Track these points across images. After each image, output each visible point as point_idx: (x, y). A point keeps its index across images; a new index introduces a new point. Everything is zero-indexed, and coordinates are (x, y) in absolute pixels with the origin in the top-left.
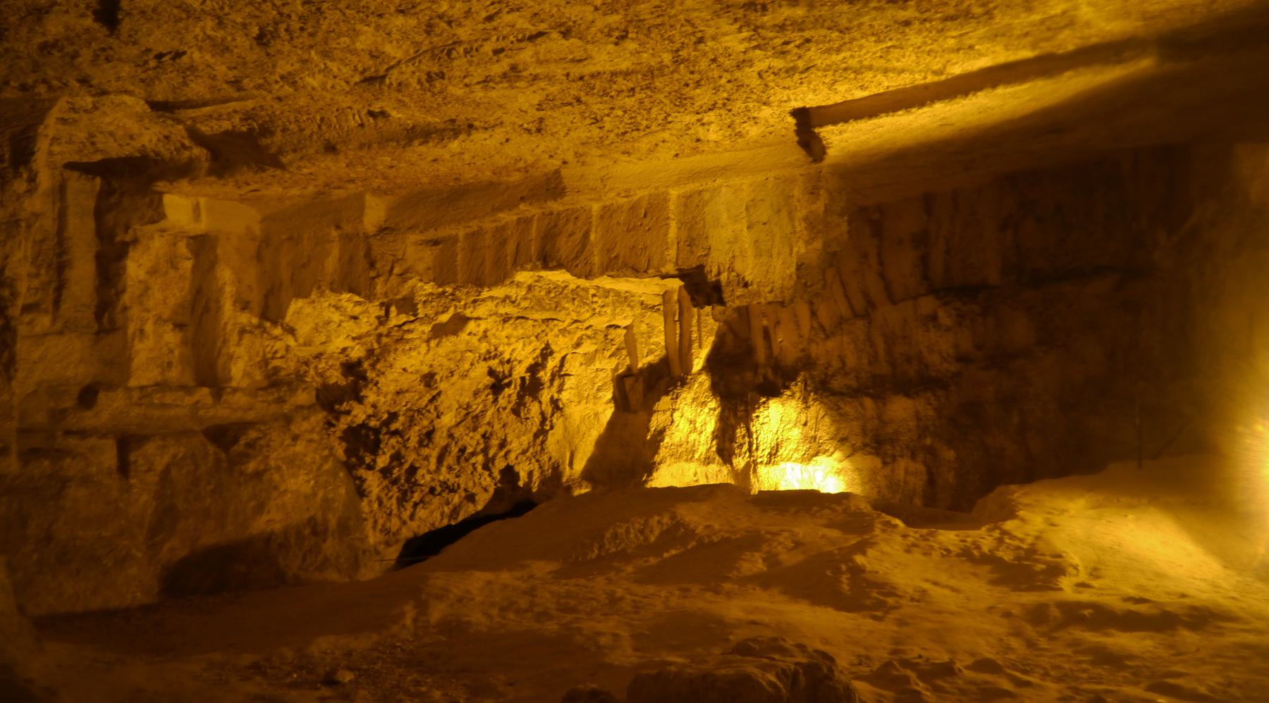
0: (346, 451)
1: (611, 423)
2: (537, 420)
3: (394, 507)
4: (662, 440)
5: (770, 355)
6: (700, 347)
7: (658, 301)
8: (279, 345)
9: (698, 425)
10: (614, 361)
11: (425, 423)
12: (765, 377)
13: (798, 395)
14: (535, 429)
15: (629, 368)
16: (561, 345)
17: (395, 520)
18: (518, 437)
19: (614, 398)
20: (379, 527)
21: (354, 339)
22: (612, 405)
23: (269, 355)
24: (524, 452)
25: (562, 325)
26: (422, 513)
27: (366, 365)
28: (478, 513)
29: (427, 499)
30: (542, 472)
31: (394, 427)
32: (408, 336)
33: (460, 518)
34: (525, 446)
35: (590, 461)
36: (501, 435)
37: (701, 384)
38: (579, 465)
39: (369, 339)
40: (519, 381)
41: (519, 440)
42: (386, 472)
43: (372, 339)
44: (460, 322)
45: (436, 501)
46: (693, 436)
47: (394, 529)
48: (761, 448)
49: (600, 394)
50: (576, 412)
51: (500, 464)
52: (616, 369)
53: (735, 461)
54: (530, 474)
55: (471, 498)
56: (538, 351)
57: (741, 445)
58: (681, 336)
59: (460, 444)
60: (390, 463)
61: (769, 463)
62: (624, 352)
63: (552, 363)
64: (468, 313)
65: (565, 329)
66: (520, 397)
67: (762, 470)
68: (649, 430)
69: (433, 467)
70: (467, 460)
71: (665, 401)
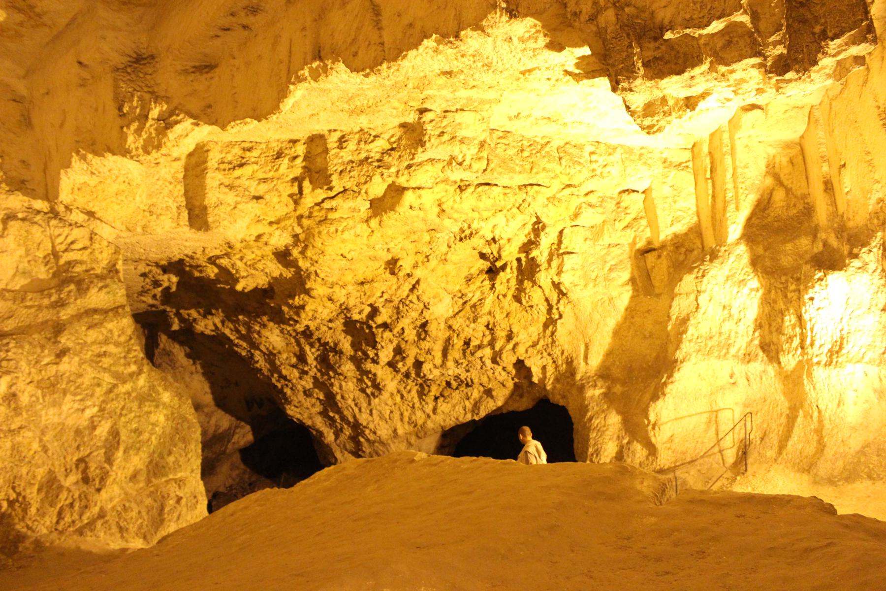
0: (353, 345)
1: (631, 311)
2: (543, 308)
3: (416, 400)
4: (685, 332)
5: (835, 213)
6: (737, 209)
7: (687, 155)
8: (76, 233)
9: (734, 312)
10: (630, 234)
11: (415, 315)
12: (825, 244)
13: (872, 266)
14: (543, 318)
15: (649, 243)
16: (555, 219)
17: (419, 413)
18: (525, 328)
19: (633, 280)
20: (406, 419)
21: (271, 223)
22: (629, 287)
23: (63, 247)
24: (534, 345)
25: (549, 193)
26: (443, 406)
27: (295, 252)
28: (499, 408)
29: (446, 394)
30: (557, 367)
31: (379, 320)
32: (331, 216)
33: (483, 413)
34: (535, 338)
35: (609, 354)
36: (505, 325)
37: (739, 257)
38: (596, 360)
39: (288, 222)
40: (515, 264)
41: (528, 331)
42: (392, 364)
43: (292, 221)
44: (396, 191)
45: (456, 395)
46: (728, 326)
47: (420, 422)
48: (817, 344)
49: (613, 275)
50: (583, 295)
51: (509, 359)
52: (634, 243)
53: (783, 359)
54: (544, 368)
55: (488, 392)
56: (529, 227)
57: (791, 338)
58: (713, 196)
59: (462, 336)
60: (394, 356)
61: (828, 364)
62: (644, 222)
63: (547, 240)
64: (402, 181)
65: (554, 197)
66: (520, 282)
67: (819, 373)
68: (669, 317)
69: (438, 361)
70: (472, 354)
71: (688, 281)
